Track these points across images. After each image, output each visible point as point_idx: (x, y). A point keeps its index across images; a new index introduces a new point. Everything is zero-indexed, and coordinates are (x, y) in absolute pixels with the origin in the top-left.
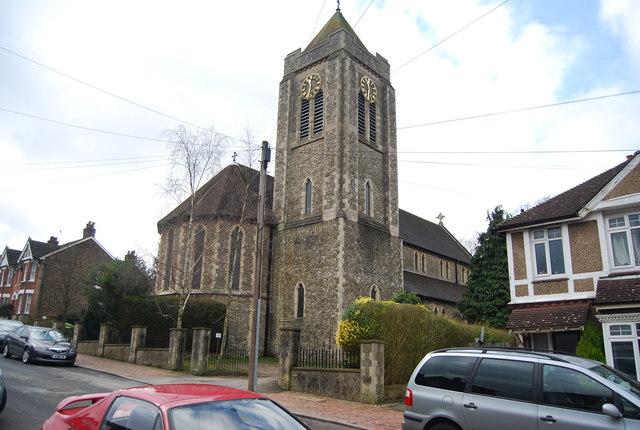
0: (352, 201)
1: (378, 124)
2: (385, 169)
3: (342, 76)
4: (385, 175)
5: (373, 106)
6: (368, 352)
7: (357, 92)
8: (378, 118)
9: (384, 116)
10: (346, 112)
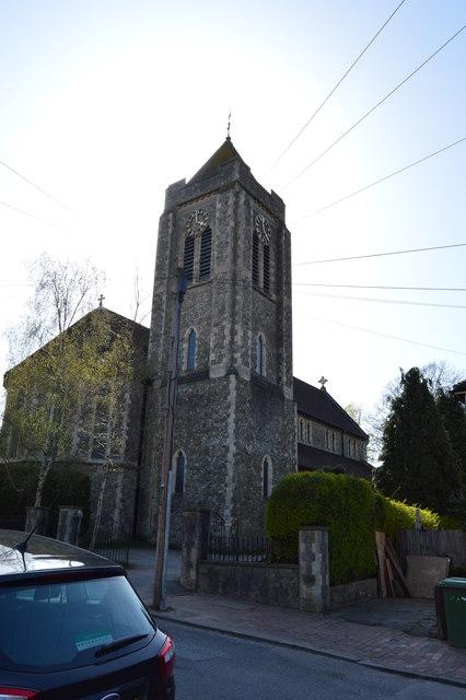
0: (244, 355)
1: (272, 270)
2: (278, 322)
3: (235, 212)
4: (279, 329)
6: (309, 540)
8: (272, 263)
10: (240, 252)
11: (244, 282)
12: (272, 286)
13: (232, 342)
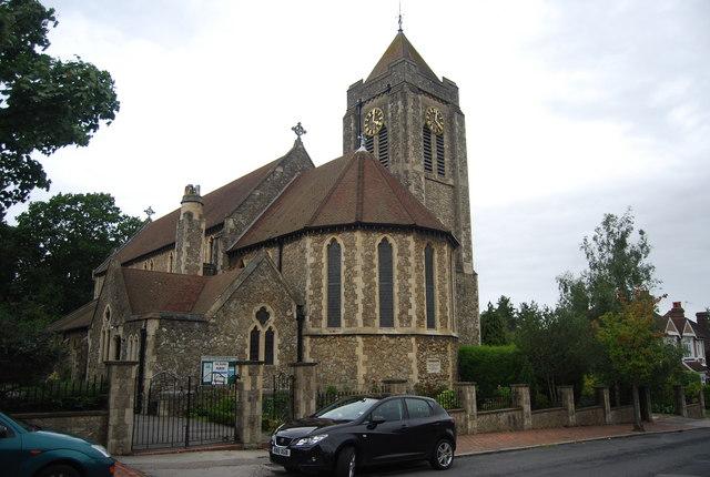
5: (440, 137)
7: (423, 124)
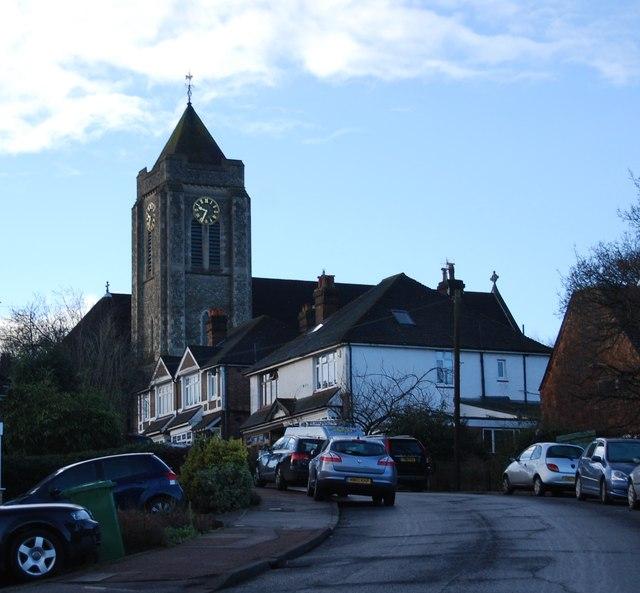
1: (223, 245)
4: (231, 301)
9: (229, 234)
11: (173, 276)
12: (223, 262)
13: (165, 332)
